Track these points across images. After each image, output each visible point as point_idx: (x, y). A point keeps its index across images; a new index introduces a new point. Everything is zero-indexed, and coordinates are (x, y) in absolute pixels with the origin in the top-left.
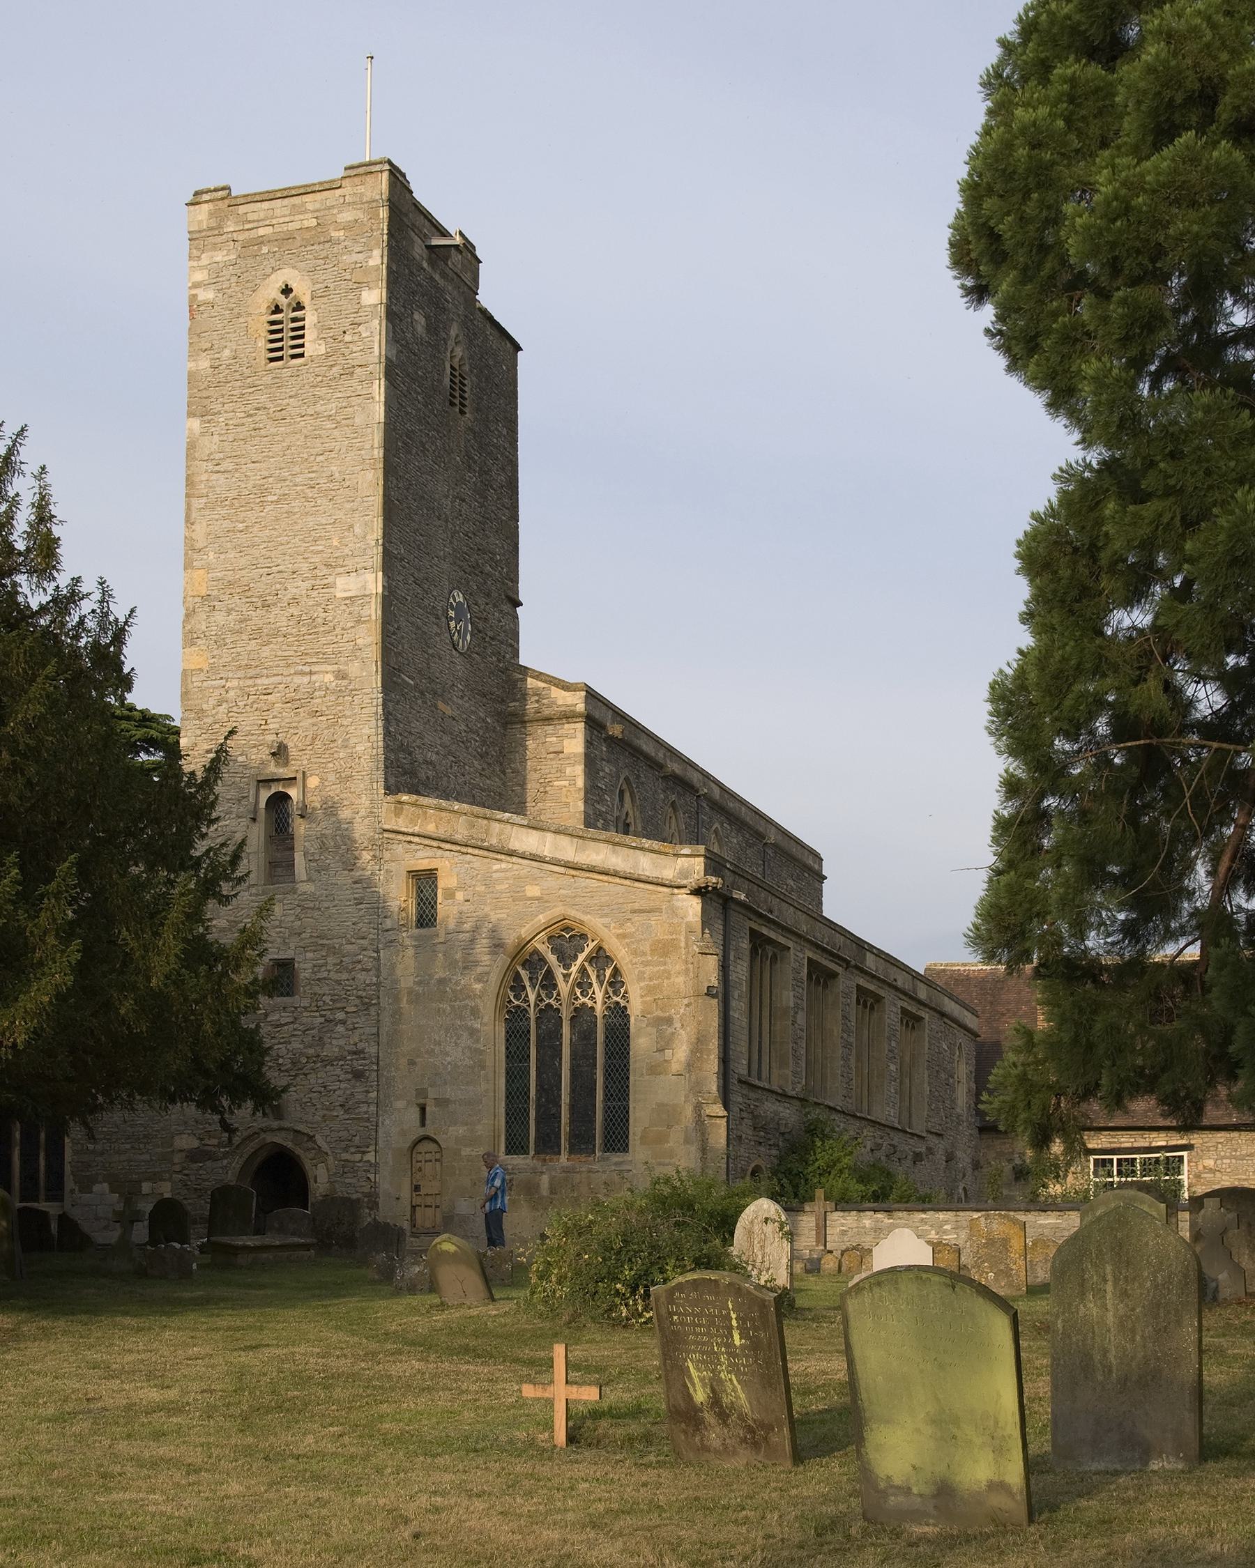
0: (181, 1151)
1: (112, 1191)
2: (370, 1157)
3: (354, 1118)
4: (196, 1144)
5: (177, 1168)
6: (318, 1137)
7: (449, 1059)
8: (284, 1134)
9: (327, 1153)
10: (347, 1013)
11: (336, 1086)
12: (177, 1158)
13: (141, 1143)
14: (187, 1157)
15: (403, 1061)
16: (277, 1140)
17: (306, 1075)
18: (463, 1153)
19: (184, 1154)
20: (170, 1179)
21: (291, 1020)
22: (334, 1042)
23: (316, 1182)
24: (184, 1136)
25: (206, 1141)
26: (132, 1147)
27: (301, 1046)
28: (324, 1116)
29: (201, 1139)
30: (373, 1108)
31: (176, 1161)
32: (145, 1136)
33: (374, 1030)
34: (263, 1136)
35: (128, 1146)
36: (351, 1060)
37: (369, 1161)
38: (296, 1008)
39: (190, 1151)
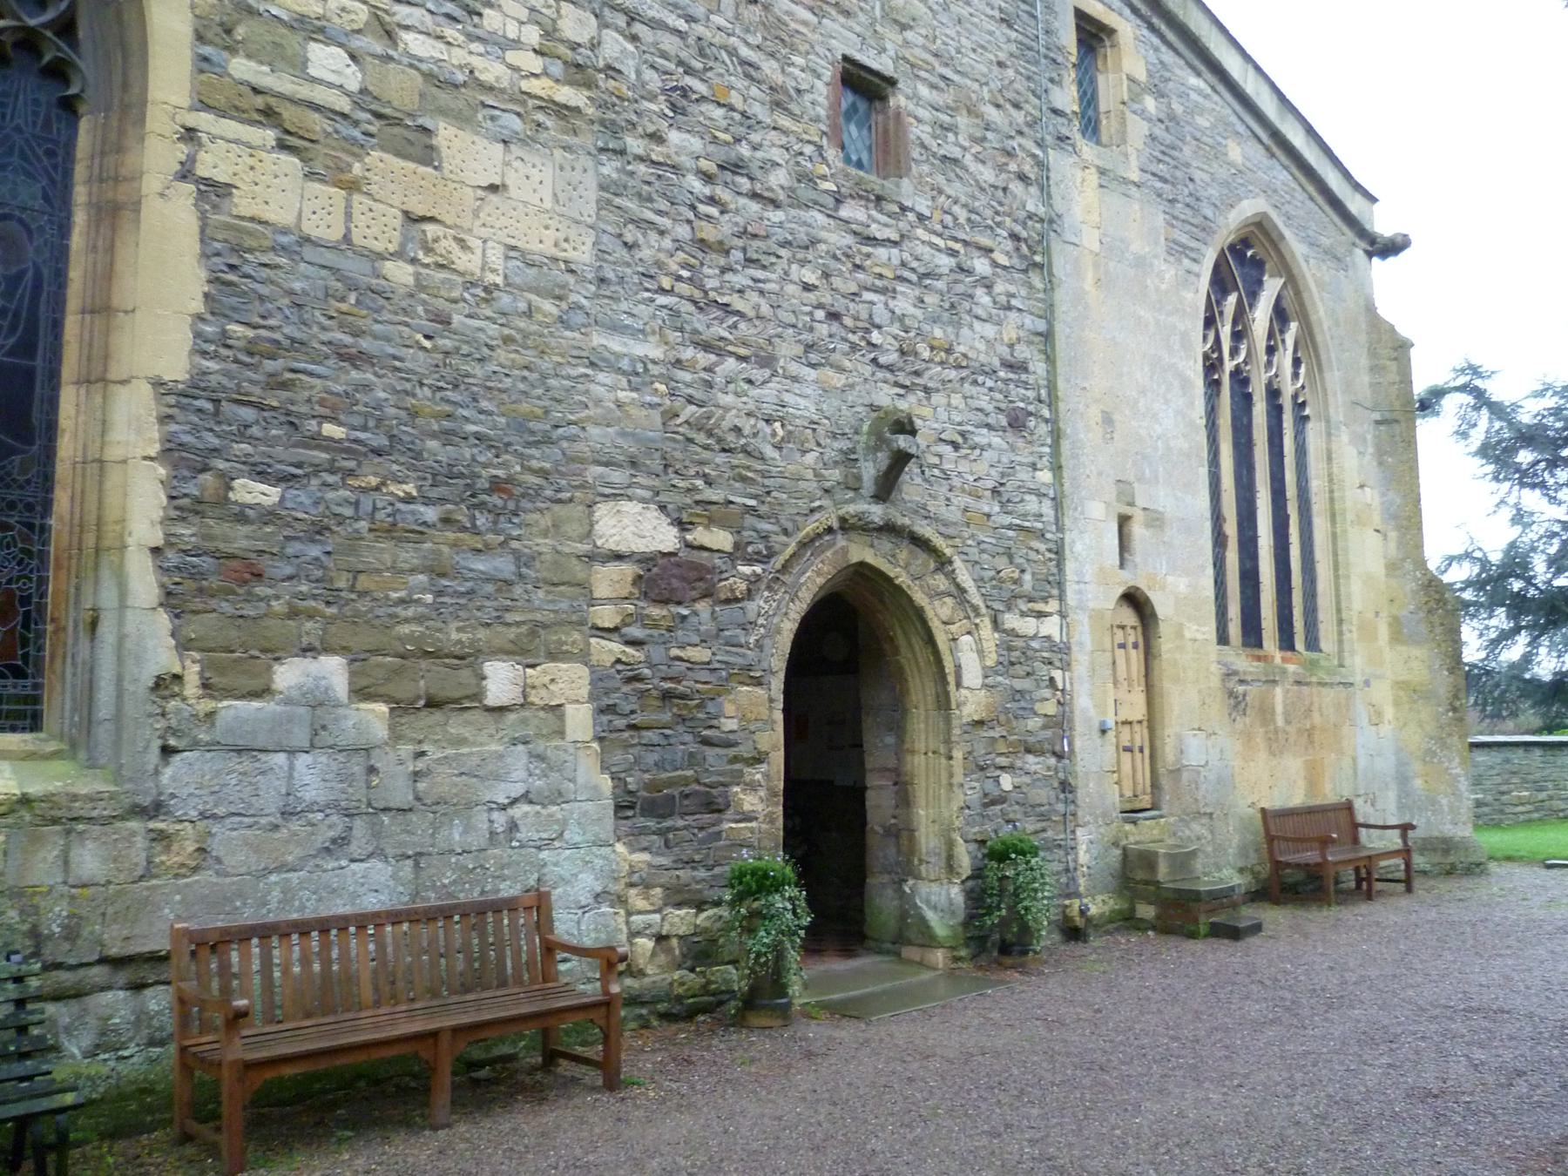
0: (618, 557)
1: (361, 693)
2: (1051, 627)
3: (1021, 528)
4: (665, 538)
5: (607, 616)
6: (958, 563)
7: (1159, 430)
8: (886, 544)
9: (976, 609)
10: (995, 264)
11: (982, 437)
12: (610, 580)
13: (481, 506)
14: (638, 579)
15: (1094, 414)
16: (870, 557)
17: (927, 390)
18: (1188, 635)
19: (629, 570)
20: (584, 657)
21: (895, 236)
22: (977, 325)
23: (959, 685)
24: (627, 506)
25: (699, 535)
26: (447, 521)
27: (918, 313)
28: (966, 510)
29: (682, 525)
30: (1047, 509)
31: (601, 591)
32: (496, 486)
33: (1041, 326)
34: (841, 541)
35: (431, 514)
36: (1006, 381)
37: (1048, 638)
38: (903, 209)
39: (646, 560)
